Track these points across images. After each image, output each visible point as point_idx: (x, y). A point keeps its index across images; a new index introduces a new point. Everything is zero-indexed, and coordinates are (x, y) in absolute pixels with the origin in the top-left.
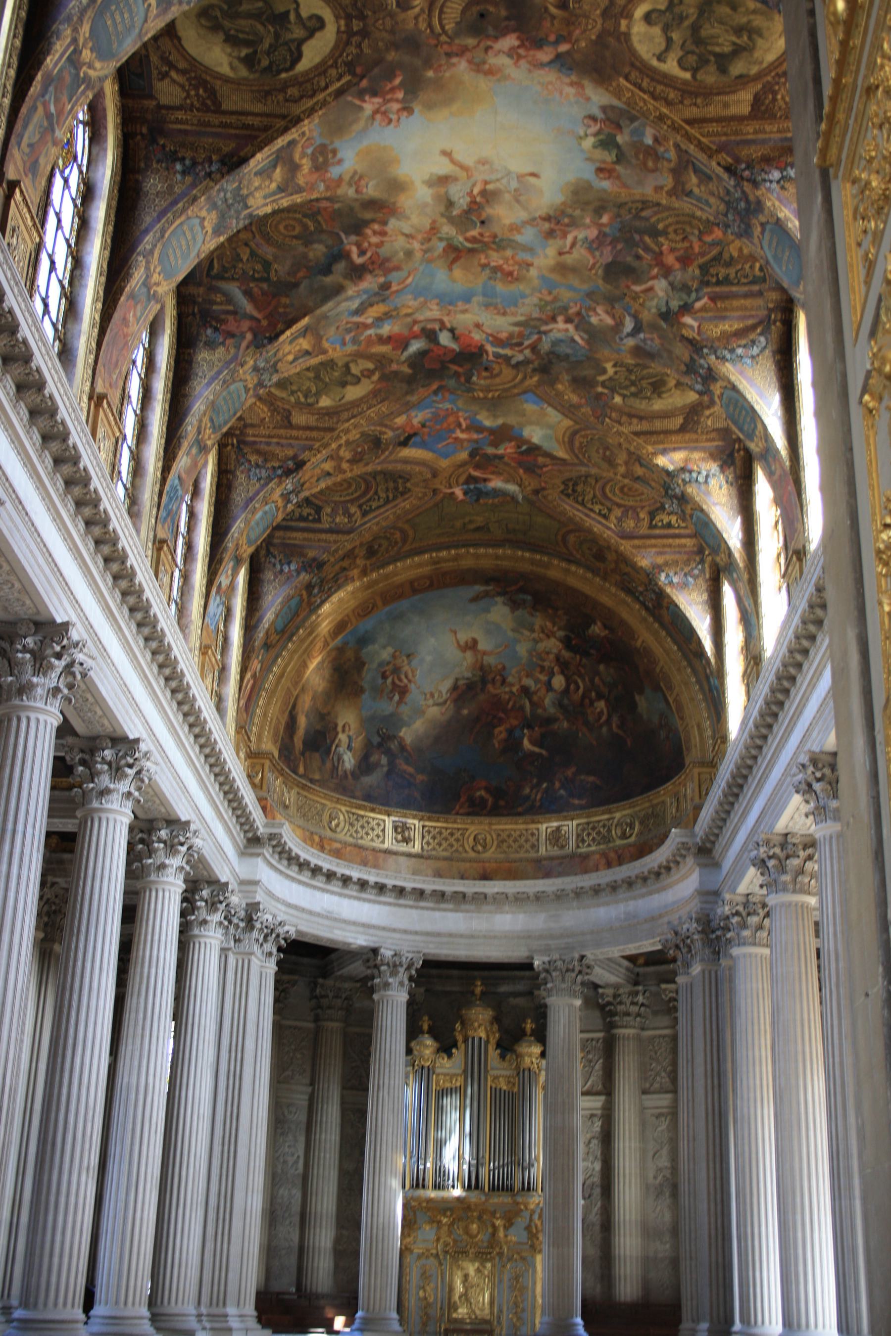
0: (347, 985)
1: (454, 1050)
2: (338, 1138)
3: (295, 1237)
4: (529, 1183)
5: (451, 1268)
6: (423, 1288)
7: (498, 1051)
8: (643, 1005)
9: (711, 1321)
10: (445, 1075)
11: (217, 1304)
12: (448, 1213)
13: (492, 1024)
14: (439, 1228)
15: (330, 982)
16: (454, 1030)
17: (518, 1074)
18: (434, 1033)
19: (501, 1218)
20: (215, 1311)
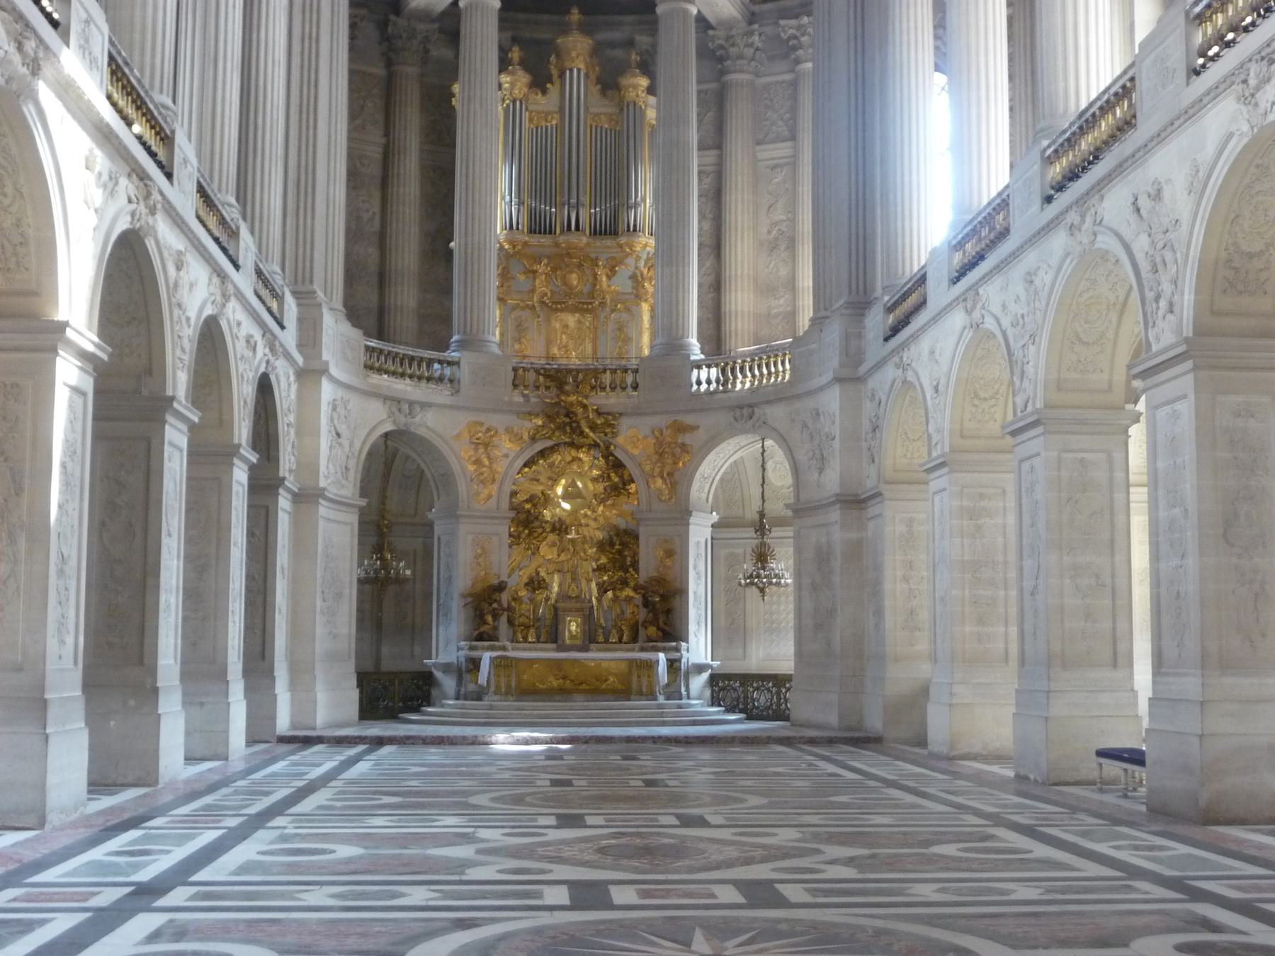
0: (421, 27)
1: (549, 85)
2: (418, 193)
3: (374, 298)
4: (635, 226)
5: (549, 320)
6: (519, 341)
7: (599, 86)
8: (757, 49)
9: (850, 292)
10: (539, 113)
11: (303, 282)
12: (545, 261)
13: (591, 57)
14: (534, 279)
15: (402, 22)
16: (549, 62)
17: (622, 110)
18: (525, 65)
19: (604, 267)
20: (300, 288)
